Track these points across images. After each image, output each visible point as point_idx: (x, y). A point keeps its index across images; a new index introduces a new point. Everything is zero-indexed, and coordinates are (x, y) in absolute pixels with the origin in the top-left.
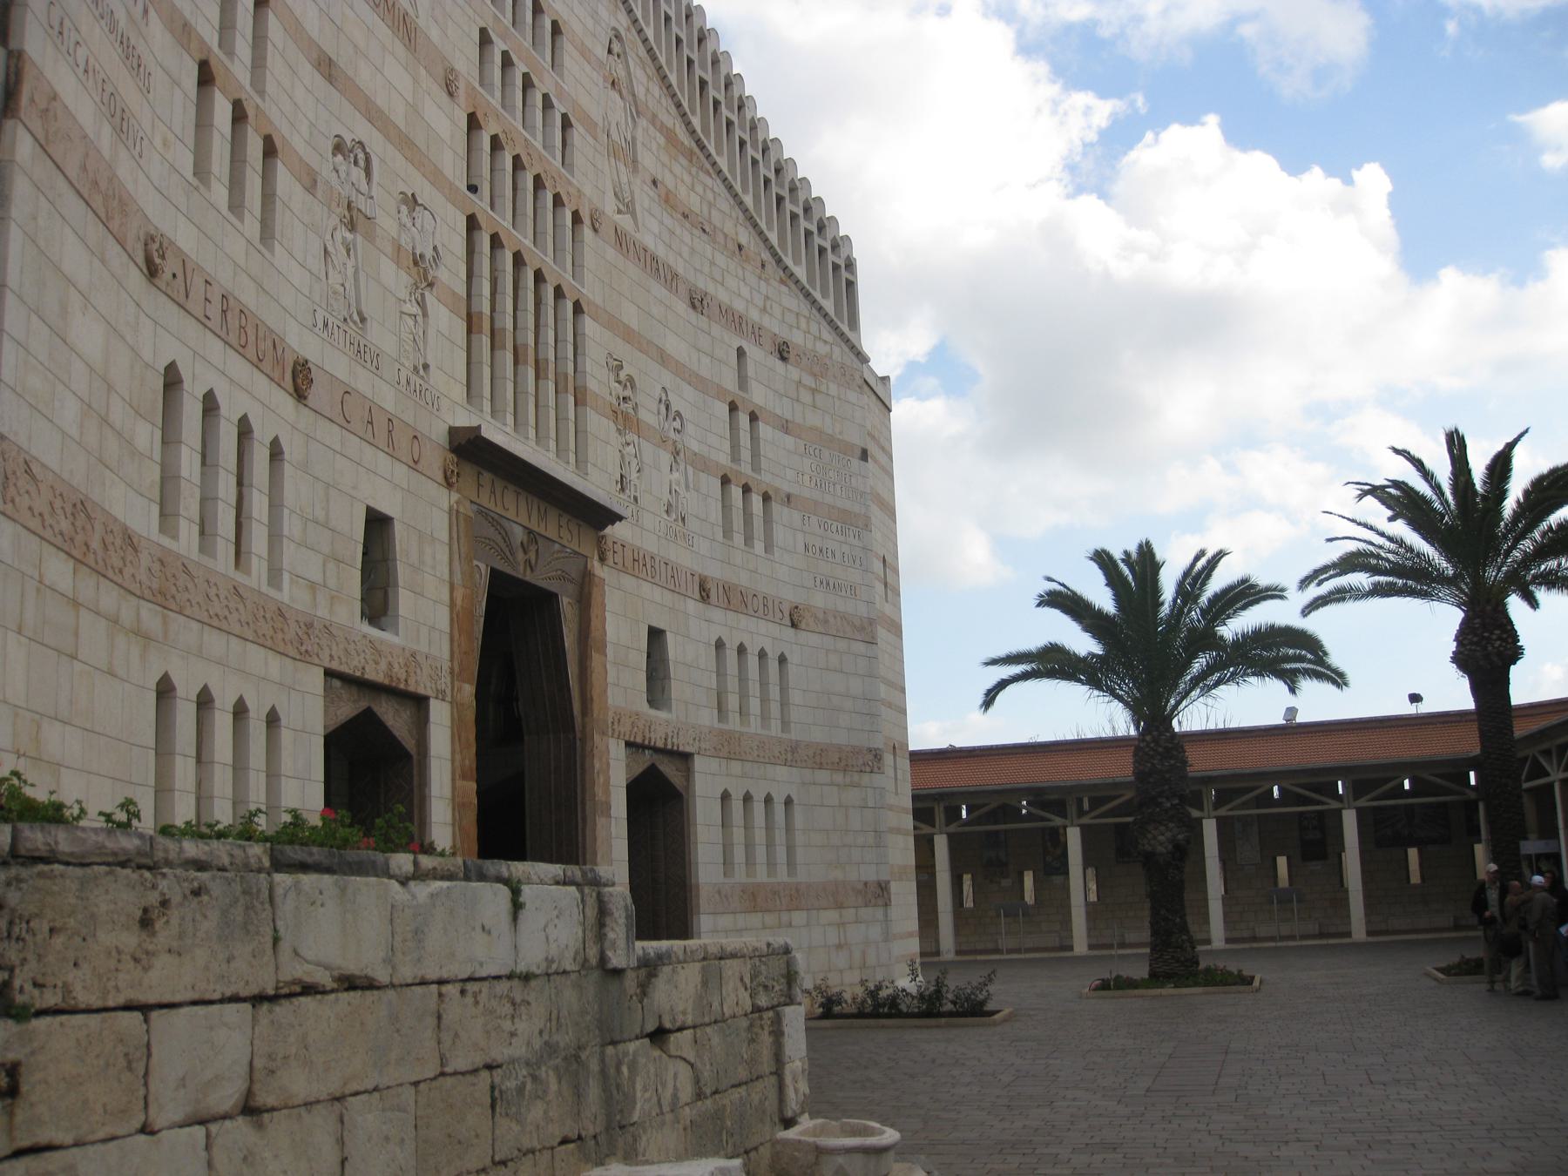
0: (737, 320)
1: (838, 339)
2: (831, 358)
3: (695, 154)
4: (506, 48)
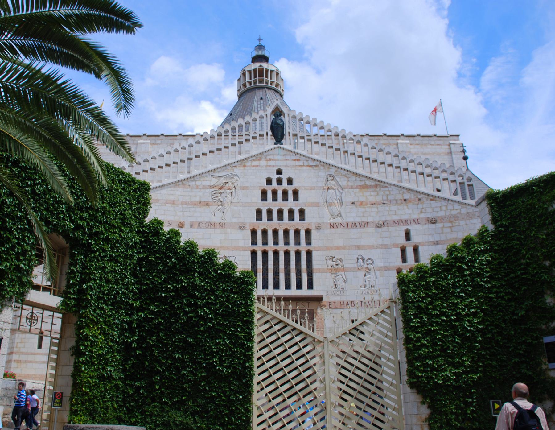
0: (404, 221)
1: (464, 206)
2: (460, 213)
3: (378, 185)
4: (268, 208)
